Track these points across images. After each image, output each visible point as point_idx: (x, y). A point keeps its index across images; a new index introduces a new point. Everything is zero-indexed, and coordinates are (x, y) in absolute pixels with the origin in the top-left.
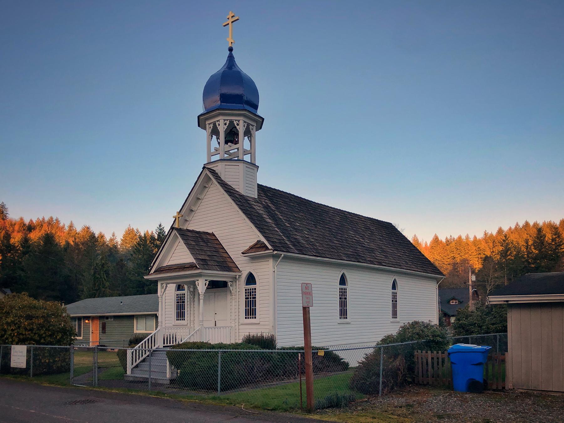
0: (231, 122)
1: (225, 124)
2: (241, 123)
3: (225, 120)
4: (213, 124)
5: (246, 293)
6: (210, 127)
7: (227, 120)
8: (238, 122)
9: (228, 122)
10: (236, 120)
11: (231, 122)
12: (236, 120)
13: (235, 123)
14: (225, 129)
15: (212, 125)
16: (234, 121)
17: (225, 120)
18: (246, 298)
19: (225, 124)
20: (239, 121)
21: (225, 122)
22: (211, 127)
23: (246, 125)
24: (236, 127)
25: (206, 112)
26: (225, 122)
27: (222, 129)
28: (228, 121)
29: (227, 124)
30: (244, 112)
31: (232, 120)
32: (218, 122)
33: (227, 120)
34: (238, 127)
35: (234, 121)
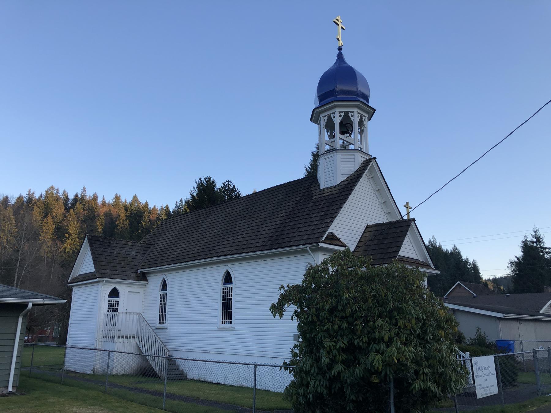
0: (346, 114)
2: (356, 114)
3: (340, 112)
4: (328, 117)
6: (325, 120)
7: (342, 112)
9: (343, 114)
10: (351, 112)
11: (346, 114)
12: (351, 112)
13: (350, 114)
15: (326, 118)
16: (349, 112)
17: (340, 112)
19: (340, 116)
20: (353, 112)
21: (340, 114)
22: (326, 120)
23: (359, 116)
24: (351, 118)
25: (320, 106)
26: (340, 114)
27: (337, 121)
28: (343, 113)
30: (359, 104)
31: (346, 111)
32: (334, 114)
33: (342, 112)
34: (352, 119)
35: (349, 112)
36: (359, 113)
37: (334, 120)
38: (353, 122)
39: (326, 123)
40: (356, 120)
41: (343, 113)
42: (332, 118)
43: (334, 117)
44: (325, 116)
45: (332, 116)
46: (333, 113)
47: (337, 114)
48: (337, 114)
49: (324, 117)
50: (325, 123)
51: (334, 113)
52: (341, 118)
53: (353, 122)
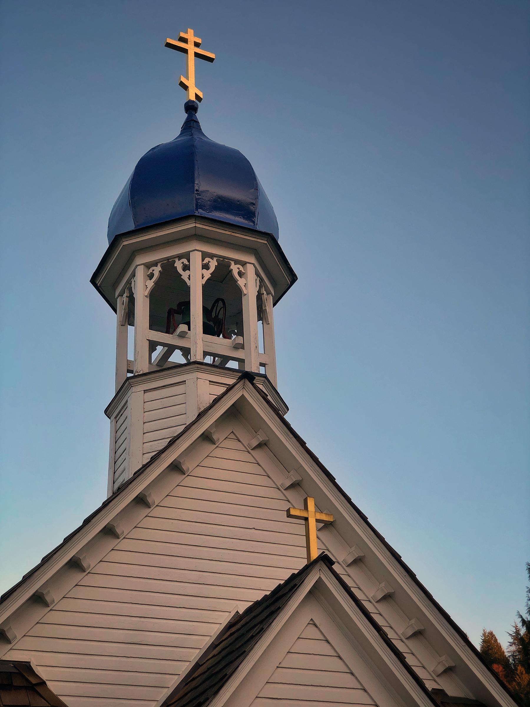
1: (206, 267)
3: (205, 255)
7: (212, 256)
8: (241, 268)
9: (213, 264)
10: (237, 262)
12: (237, 262)
13: (235, 268)
14: (206, 279)
17: (205, 255)
19: (206, 267)
21: (207, 260)
24: (236, 281)
28: (215, 259)
29: (212, 269)
31: (224, 258)
33: (212, 256)
34: (241, 282)
35: (233, 263)
37: (184, 275)
38: (245, 292)
41: (215, 259)
43: (186, 268)
44: (155, 264)
45: (179, 265)
46: (180, 257)
47: (196, 260)
48: (196, 260)
49: (148, 266)
50: (151, 284)
51: (187, 256)
53: (245, 291)
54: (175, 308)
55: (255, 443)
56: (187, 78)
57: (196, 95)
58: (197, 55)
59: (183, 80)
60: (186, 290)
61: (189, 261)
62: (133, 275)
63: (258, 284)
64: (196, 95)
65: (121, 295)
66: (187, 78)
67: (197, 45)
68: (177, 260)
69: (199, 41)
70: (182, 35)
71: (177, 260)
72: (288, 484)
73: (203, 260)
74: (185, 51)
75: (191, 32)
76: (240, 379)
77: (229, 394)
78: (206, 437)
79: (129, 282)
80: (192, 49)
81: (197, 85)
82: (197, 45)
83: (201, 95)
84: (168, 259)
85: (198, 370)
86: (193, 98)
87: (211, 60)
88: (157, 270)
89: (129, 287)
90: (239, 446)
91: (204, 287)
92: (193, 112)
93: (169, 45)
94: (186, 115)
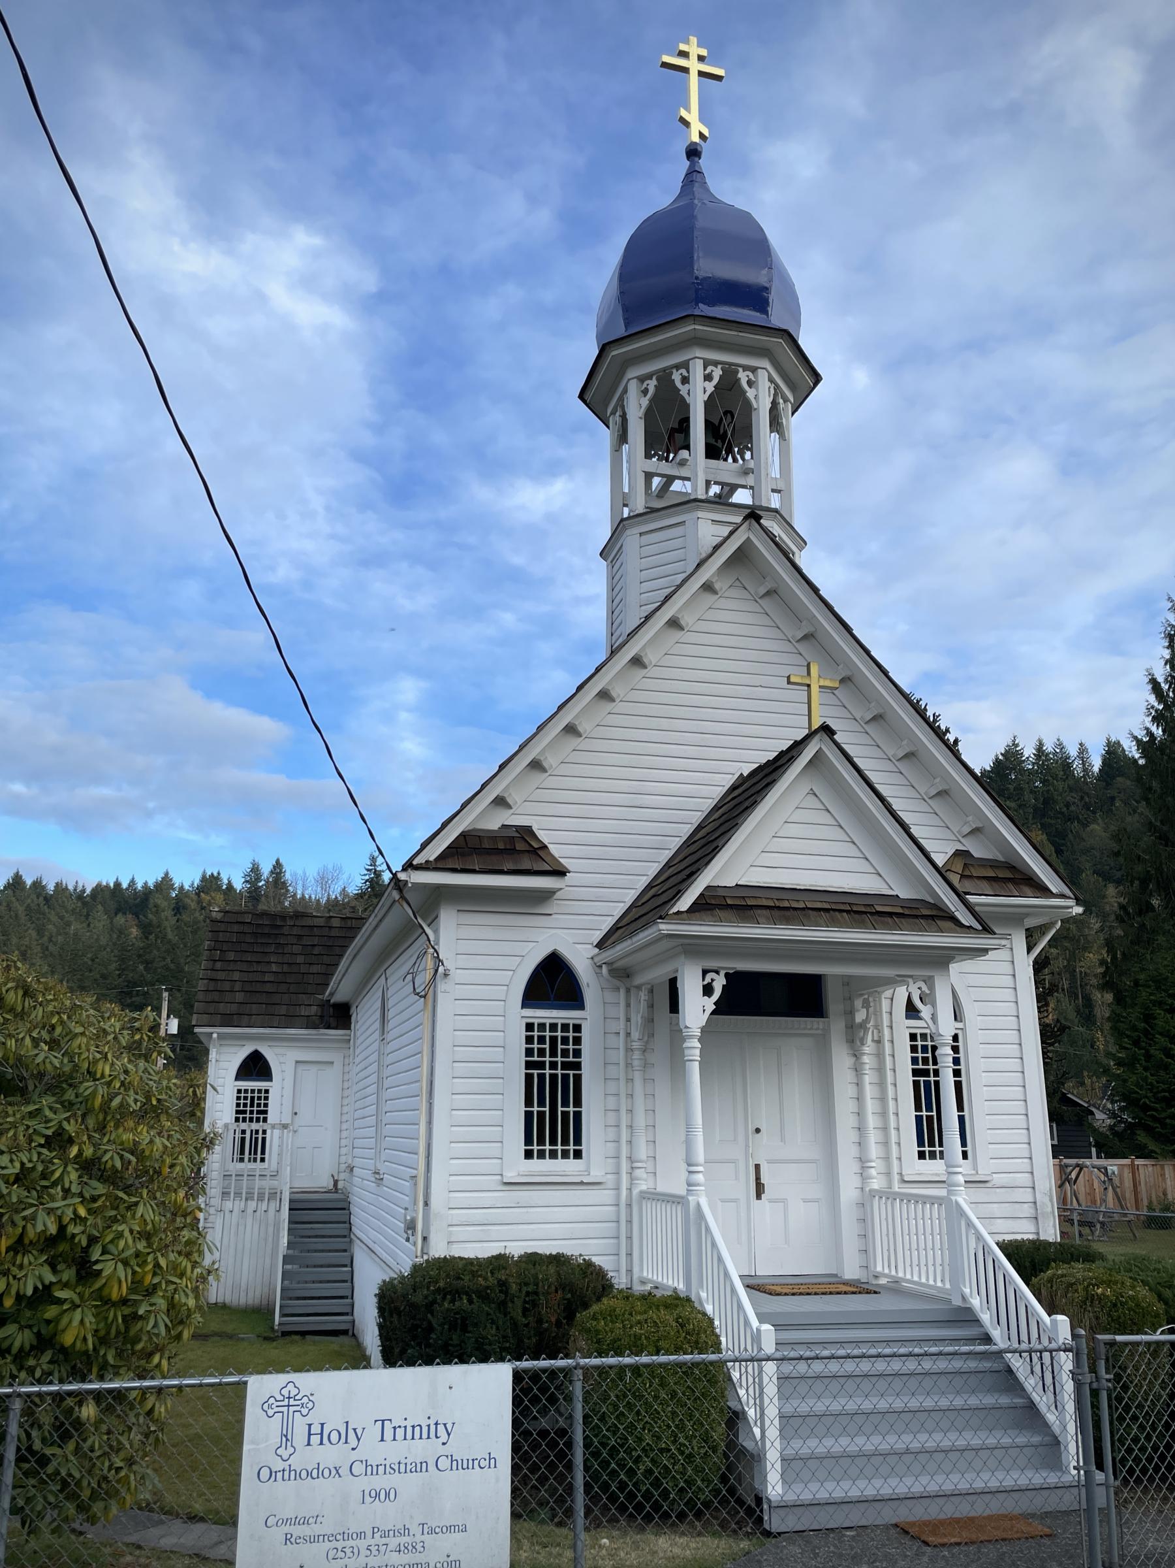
1: (708, 378)
5: (914, 1049)
7: (715, 363)
8: (751, 376)
9: (717, 373)
10: (746, 368)
12: (746, 368)
13: (743, 376)
18: (916, 1073)
19: (708, 378)
20: (754, 370)
24: (744, 392)
31: (731, 364)
33: (715, 363)
34: (750, 393)
35: (741, 370)
36: (771, 380)
37: (683, 390)
38: (755, 405)
39: (651, 401)
40: (761, 397)
42: (678, 384)
43: (685, 380)
44: (649, 376)
45: (676, 377)
46: (677, 367)
49: (642, 379)
50: (645, 402)
51: (685, 365)
52: (710, 387)
54: (676, 426)
55: (762, 591)
56: (689, 111)
57: (701, 135)
58: (701, 74)
59: (683, 113)
60: (685, 407)
61: (688, 372)
62: (625, 391)
63: (772, 391)
64: (701, 135)
65: (613, 413)
66: (689, 111)
67: (701, 59)
68: (674, 371)
69: (704, 52)
70: (683, 47)
71: (674, 371)
72: (800, 635)
73: (705, 369)
74: (685, 70)
75: (694, 40)
76: (746, 518)
77: (732, 537)
78: (708, 587)
79: (621, 399)
80: (694, 66)
81: (702, 119)
82: (701, 59)
83: (706, 132)
84: (664, 370)
85: (698, 509)
86: (695, 138)
87: (719, 78)
88: (652, 384)
89: (621, 404)
90: (745, 594)
91: (706, 403)
92: (696, 159)
93: (665, 65)
94: (688, 163)
